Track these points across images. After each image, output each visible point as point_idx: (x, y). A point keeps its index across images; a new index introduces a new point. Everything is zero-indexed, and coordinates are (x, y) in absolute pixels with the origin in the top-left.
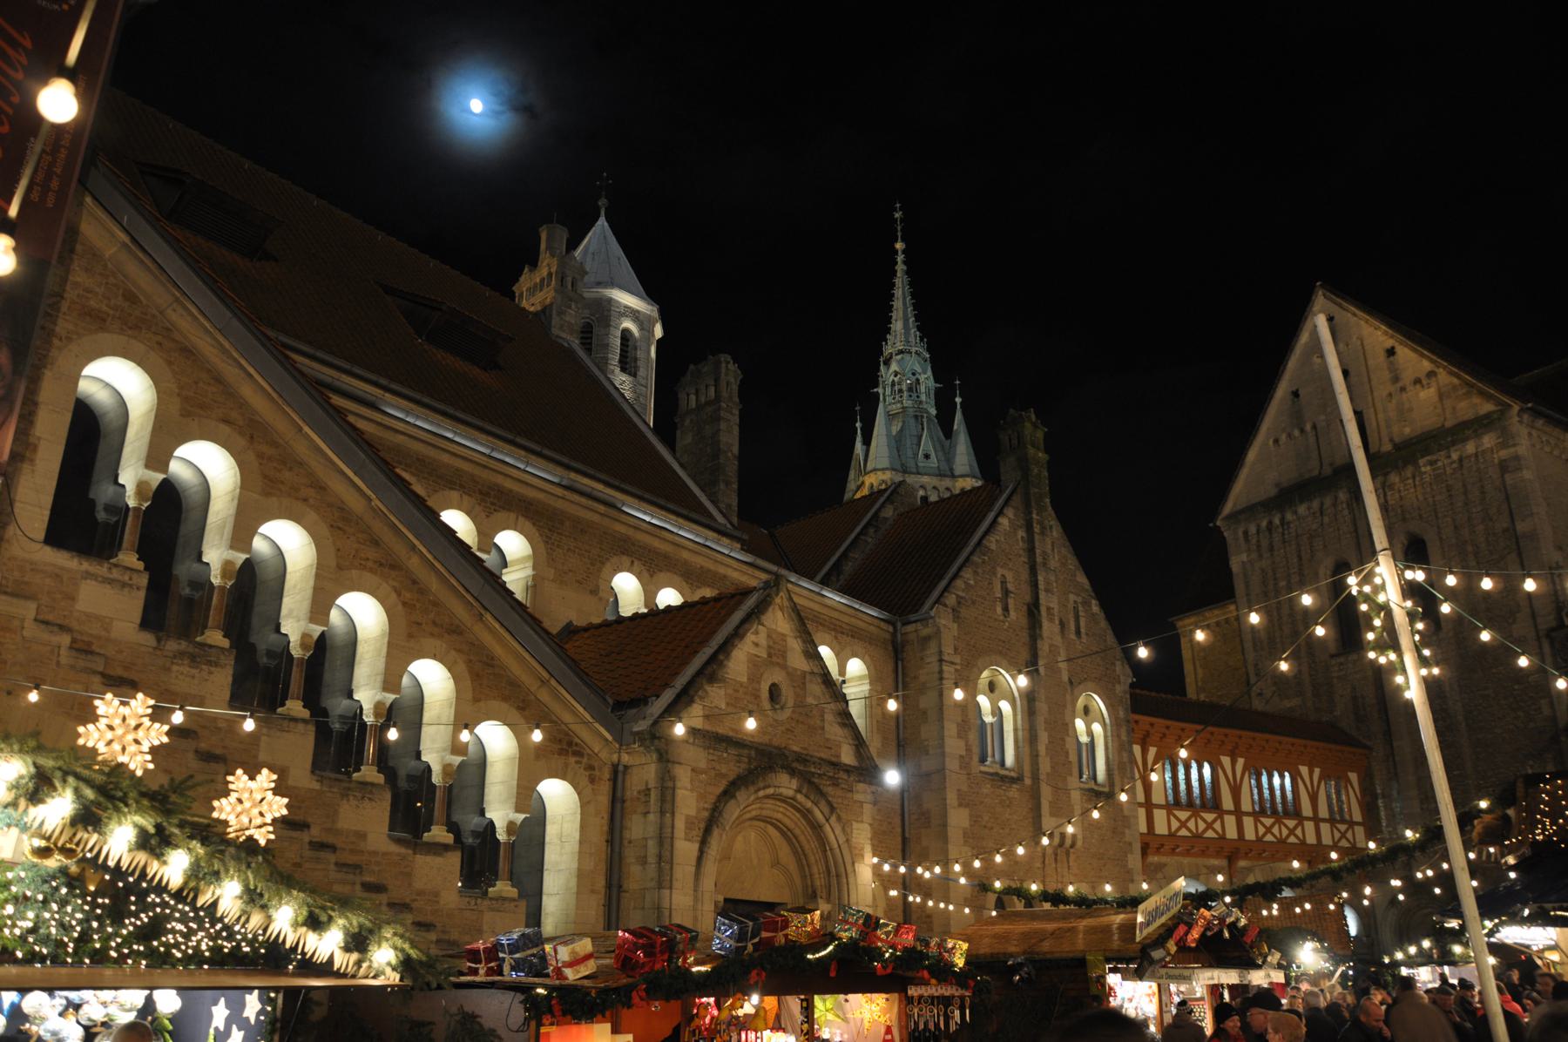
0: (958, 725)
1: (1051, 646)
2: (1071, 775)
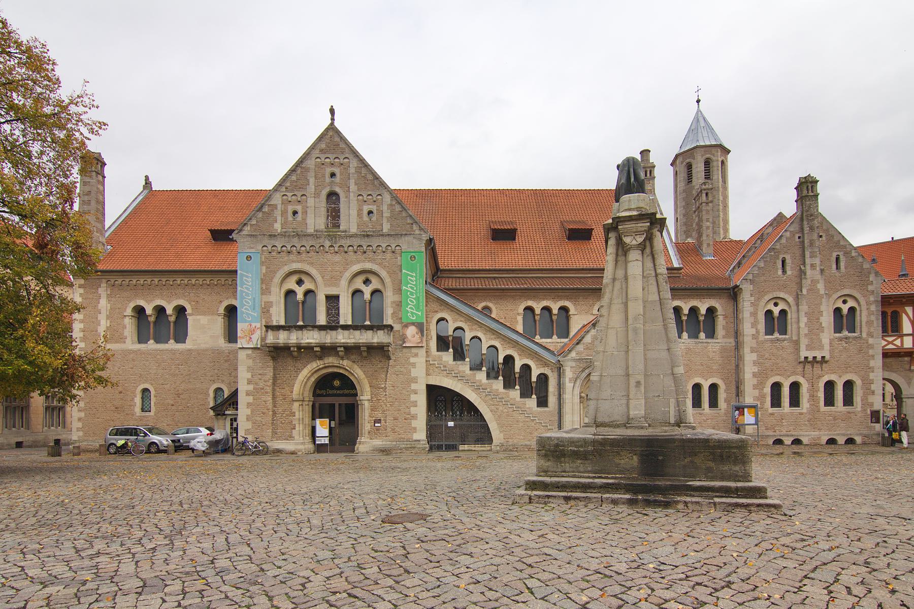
0: (752, 323)
2: (823, 332)
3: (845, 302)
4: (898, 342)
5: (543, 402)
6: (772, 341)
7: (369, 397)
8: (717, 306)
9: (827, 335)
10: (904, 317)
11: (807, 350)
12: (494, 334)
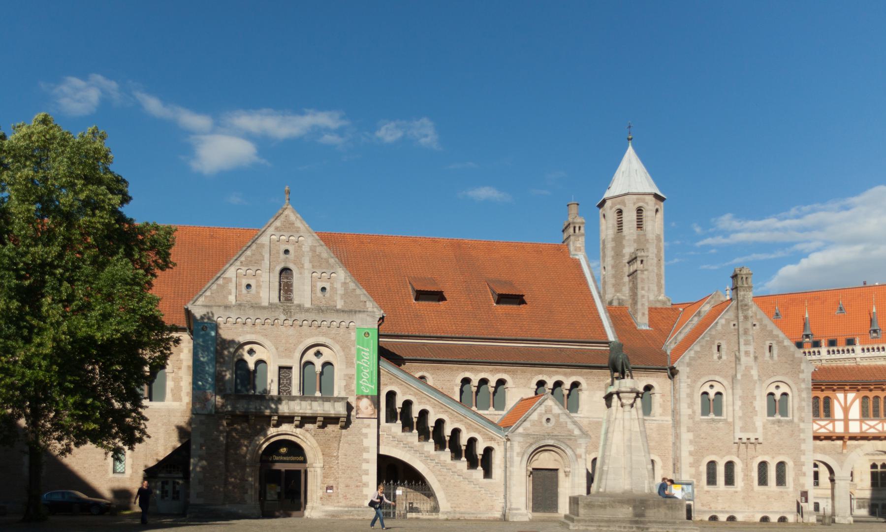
0: (688, 404)
1: (746, 367)
2: (756, 415)
3: (777, 387)
4: (830, 427)
5: (488, 474)
6: (708, 422)
7: (322, 465)
9: (761, 417)
10: (836, 403)
11: (741, 432)
12: (442, 408)
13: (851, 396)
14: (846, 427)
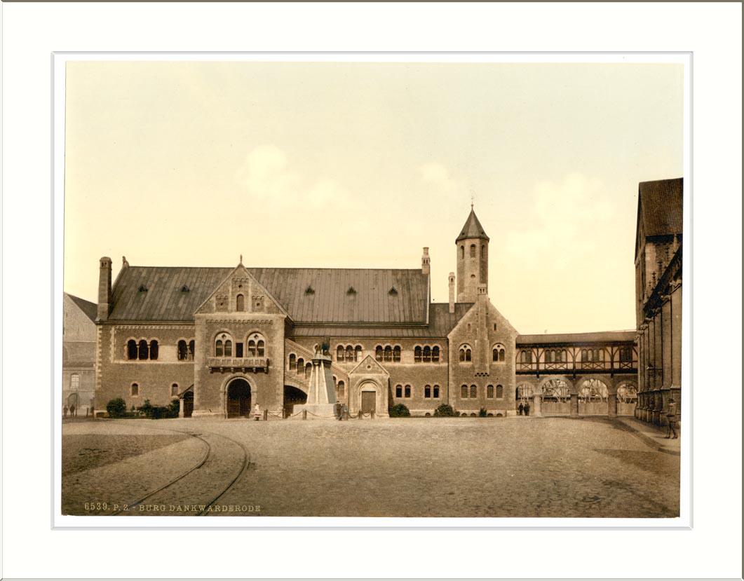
4: (530, 367)
8: (439, 346)
13: (541, 350)
14: (538, 366)
